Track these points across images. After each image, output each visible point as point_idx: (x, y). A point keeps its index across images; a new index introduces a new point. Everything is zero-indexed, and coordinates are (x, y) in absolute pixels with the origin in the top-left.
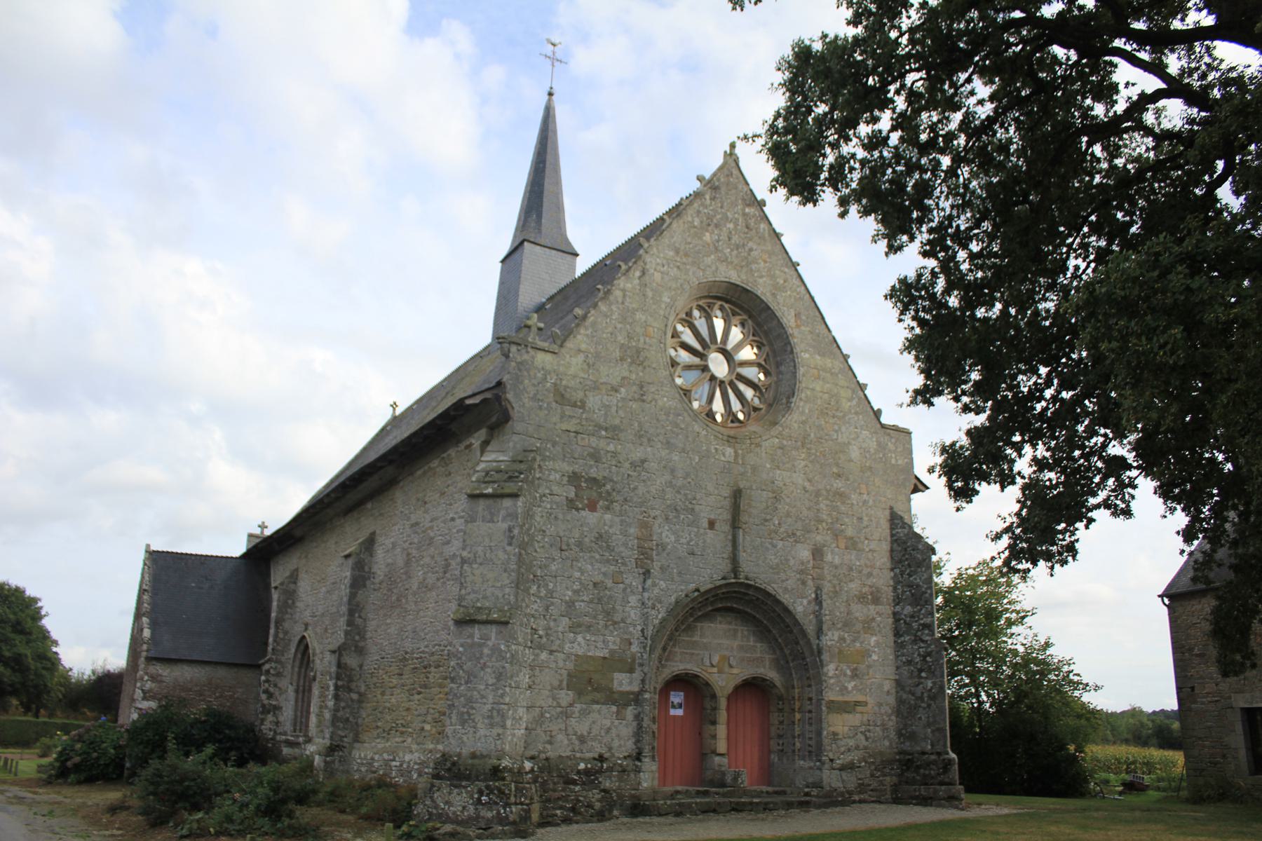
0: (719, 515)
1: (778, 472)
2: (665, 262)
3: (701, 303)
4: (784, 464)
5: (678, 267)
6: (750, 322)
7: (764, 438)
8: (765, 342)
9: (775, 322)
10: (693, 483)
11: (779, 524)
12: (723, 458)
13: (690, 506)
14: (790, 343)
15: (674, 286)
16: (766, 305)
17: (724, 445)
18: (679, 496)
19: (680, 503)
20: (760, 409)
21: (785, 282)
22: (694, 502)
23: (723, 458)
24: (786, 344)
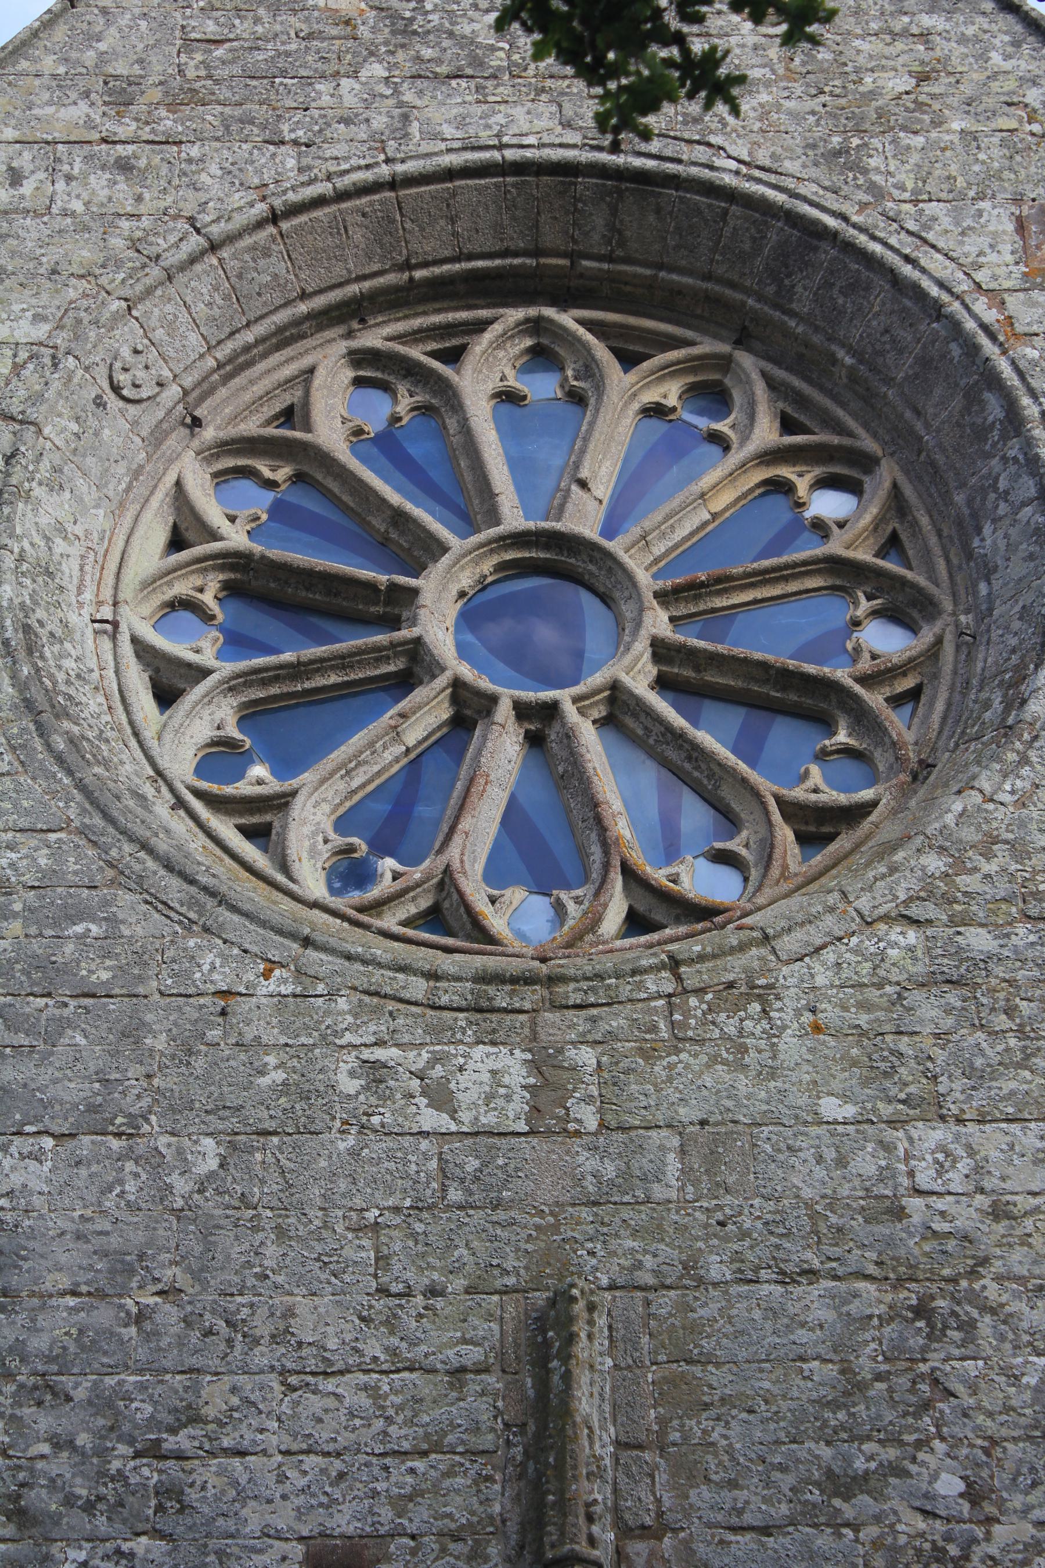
0: (402, 1503)
1: (937, 1134)
2: (25, 160)
3: (373, 339)
4: (977, 1076)
5: (124, 166)
6: (746, 361)
7: (788, 944)
8: (869, 444)
9: (880, 296)
10: (169, 1315)
11: (973, 1494)
12: (431, 1119)
13: (149, 1474)
14: (993, 380)
15: (85, 253)
16: (792, 218)
17: (436, 1032)
18: (44, 1422)
19: (61, 1465)
20: (865, 809)
21: (923, 78)
22: (183, 1440)
23: (431, 1119)
24: (973, 399)
